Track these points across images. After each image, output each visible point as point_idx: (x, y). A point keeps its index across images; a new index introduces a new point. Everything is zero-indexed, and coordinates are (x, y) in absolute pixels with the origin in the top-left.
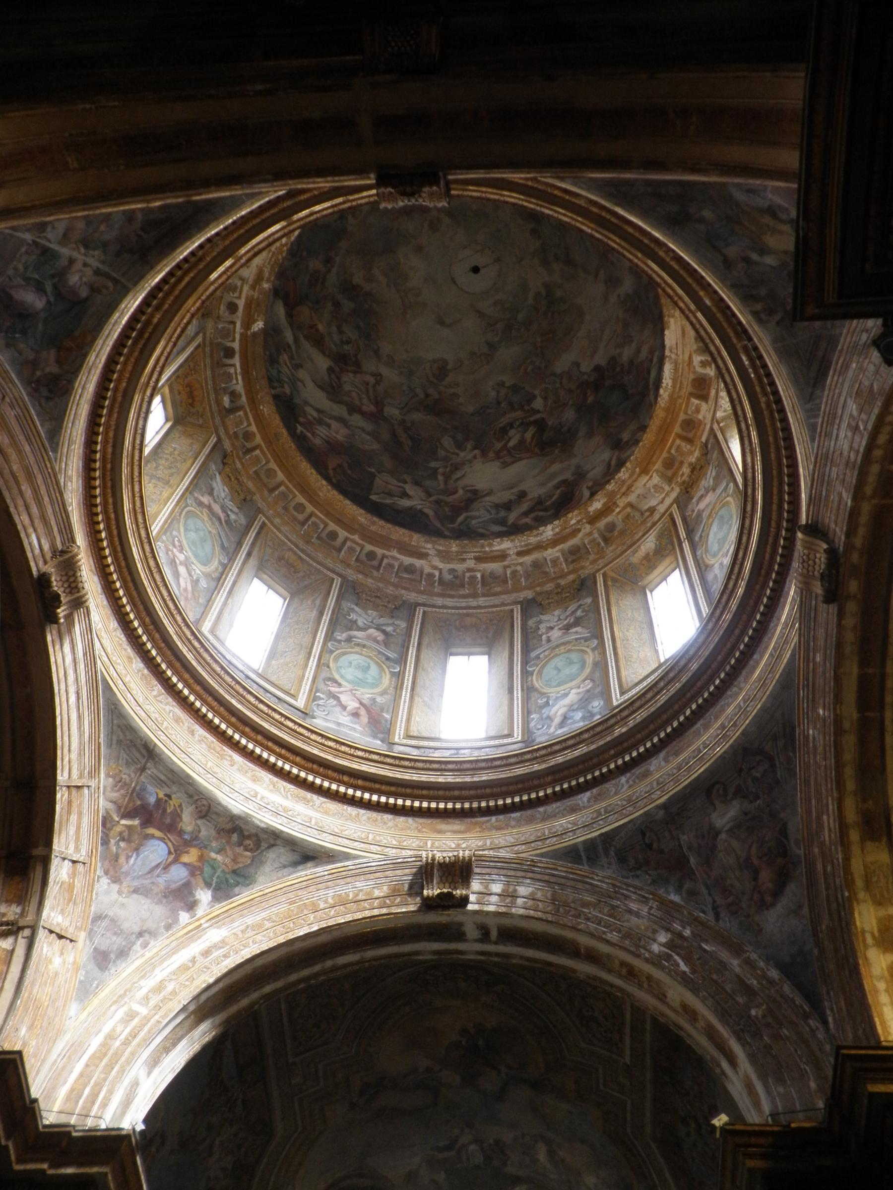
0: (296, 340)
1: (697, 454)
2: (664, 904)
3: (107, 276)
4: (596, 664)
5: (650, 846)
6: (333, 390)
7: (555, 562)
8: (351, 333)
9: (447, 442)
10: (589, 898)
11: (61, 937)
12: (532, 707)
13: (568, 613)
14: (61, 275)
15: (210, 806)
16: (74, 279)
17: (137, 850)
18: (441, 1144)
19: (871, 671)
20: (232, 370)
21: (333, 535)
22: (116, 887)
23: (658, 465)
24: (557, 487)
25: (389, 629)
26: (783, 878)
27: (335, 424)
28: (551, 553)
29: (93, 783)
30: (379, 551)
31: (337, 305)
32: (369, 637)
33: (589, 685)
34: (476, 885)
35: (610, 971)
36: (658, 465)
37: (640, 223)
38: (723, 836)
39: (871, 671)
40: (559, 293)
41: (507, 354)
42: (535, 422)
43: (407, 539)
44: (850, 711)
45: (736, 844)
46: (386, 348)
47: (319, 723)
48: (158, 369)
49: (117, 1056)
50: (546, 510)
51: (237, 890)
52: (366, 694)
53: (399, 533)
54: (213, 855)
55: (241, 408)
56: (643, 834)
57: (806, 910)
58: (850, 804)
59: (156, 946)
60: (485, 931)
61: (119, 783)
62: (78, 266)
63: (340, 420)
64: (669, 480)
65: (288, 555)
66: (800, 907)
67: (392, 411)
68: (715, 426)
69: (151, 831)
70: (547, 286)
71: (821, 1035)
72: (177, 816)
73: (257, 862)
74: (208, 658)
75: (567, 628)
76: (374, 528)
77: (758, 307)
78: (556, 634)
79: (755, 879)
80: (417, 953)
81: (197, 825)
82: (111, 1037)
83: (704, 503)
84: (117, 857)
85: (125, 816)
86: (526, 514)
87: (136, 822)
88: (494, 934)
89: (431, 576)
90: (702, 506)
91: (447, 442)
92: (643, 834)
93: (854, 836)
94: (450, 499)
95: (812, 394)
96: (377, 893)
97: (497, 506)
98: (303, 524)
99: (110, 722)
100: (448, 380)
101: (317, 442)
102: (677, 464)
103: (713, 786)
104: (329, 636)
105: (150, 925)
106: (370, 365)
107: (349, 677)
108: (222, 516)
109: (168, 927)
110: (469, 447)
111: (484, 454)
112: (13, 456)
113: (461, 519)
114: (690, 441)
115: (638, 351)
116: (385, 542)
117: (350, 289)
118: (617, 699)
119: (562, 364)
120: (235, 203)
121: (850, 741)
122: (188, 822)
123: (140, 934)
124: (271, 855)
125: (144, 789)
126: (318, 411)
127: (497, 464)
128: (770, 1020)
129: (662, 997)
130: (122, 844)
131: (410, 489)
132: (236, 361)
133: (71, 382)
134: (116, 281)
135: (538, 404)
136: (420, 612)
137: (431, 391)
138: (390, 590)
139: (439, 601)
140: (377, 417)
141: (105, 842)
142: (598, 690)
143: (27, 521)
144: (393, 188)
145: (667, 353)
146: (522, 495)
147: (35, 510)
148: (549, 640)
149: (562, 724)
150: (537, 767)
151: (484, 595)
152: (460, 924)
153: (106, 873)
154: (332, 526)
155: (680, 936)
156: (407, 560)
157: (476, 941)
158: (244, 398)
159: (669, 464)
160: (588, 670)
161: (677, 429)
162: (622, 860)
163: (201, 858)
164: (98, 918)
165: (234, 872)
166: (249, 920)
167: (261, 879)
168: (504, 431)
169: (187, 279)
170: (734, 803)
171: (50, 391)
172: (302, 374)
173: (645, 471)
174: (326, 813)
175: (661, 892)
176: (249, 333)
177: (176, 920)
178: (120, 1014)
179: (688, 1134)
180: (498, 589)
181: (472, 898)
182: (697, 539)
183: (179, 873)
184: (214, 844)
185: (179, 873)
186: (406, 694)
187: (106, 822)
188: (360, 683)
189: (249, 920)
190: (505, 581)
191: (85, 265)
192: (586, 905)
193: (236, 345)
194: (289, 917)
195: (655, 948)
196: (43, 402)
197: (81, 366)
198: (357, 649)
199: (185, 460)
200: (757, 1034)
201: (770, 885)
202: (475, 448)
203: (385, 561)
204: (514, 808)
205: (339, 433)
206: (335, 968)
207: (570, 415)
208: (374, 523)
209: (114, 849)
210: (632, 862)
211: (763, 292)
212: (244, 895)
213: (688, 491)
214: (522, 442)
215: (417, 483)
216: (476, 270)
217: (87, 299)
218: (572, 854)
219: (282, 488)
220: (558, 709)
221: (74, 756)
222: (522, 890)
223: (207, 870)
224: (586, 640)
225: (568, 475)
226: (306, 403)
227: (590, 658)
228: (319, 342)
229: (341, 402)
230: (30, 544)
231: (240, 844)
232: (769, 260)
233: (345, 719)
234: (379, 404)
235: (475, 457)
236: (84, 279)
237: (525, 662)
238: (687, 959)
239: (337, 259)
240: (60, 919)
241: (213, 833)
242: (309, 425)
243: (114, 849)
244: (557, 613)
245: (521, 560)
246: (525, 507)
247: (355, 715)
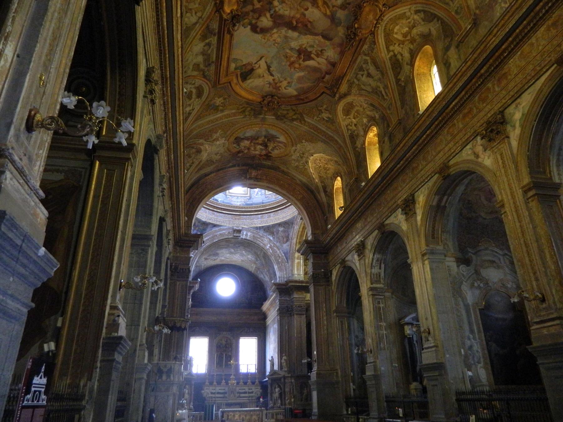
2: (270, 239)
10: (259, 237)
26: (287, 241)
34: (242, 233)
44: (301, 230)
58: (298, 240)
121: (300, 233)
162: (264, 230)
167: (208, 230)
192: (258, 238)
194: (213, 237)
200: (279, 264)
218: (257, 228)
222: (249, 234)
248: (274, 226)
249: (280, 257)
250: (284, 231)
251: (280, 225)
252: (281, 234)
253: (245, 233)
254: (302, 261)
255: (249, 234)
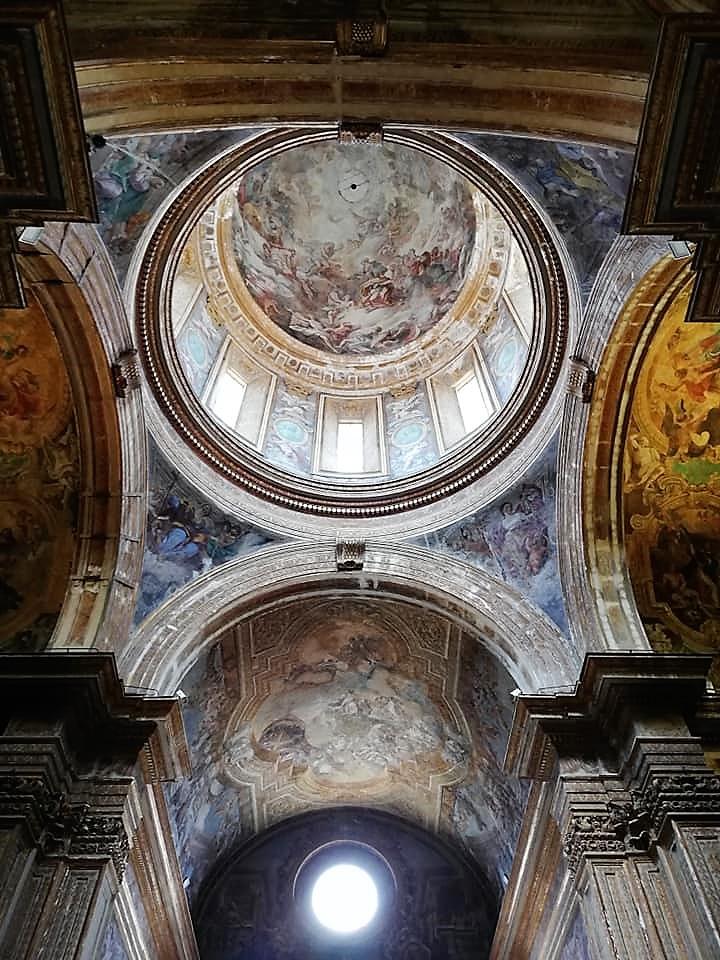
0: (244, 224)
1: (491, 310)
2: (474, 569)
3: (161, 176)
4: (429, 432)
5: (466, 537)
6: (267, 259)
7: (401, 371)
8: (277, 223)
9: (334, 295)
11: (124, 585)
12: (392, 456)
13: (411, 400)
14: (134, 173)
15: (211, 509)
16: (140, 177)
17: (168, 534)
18: (335, 702)
19: (605, 442)
20: (212, 242)
21: (271, 349)
22: (155, 556)
23: (466, 315)
24: (400, 326)
25: (305, 407)
26: (544, 558)
27: (268, 280)
28: (399, 366)
29: (142, 495)
30: (298, 361)
31: (269, 204)
32: (295, 411)
33: (425, 444)
35: (443, 608)
36: (466, 315)
37: (495, 164)
38: (509, 533)
39: (605, 442)
40: (404, 205)
41: (371, 242)
42: (386, 286)
43: (314, 354)
44: (592, 466)
45: (516, 538)
46: (297, 234)
47: (269, 461)
48: (184, 239)
49: (161, 654)
50: (393, 340)
51: (227, 559)
52: (295, 445)
53: (309, 350)
54: (213, 538)
55: (217, 267)
56: (462, 531)
57: (558, 575)
58: (589, 517)
59: (180, 591)
60: (371, 586)
61: (157, 495)
62: (143, 168)
63: (271, 278)
64: (472, 325)
65: (245, 360)
66: (554, 575)
67: (301, 274)
68: (504, 293)
69: (176, 523)
70: (397, 200)
71: (567, 646)
72: (191, 515)
73: (239, 542)
74: (209, 421)
75: (410, 410)
76: (295, 346)
77: (562, 222)
78: (403, 414)
79: (528, 558)
80: (331, 595)
81: (203, 520)
82: (157, 643)
83: (495, 339)
84: (156, 538)
85: (159, 515)
86: (382, 342)
87: (167, 518)
88: (376, 585)
89: (328, 376)
90: (493, 341)
91: (334, 295)
92: (462, 531)
93: (591, 536)
94: (336, 330)
95: (588, 277)
96: (309, 561)
97: (364, 336)
98: (253, 341)
99: (152, 458)
100: (333, 257)
101: (258, 291)
102: (476, 316)
103: (503, 506)
104: (272, 410)
105: (175, 579)
106: (288, 244)
107: (285, 435)
108: (208, 334)
109: (186, 581)
110: (347, 299)
111: (356, 303)
112: (99, 292)
113: (342, 343)
114: (485, 301)
115: (452, 244)
116: (302, 356)
117: (277, 195)
118: (442, 453)
119: (403, 251)
120: (246, 134)
121: (591, 483)
122: (198, 518)
123: (170, 584)
124: (248, 537)
125: (172, 499)
126: (259, 272)
127: (364, 310)
128: (537, 637)
129: (473, 624)
130: (159, 531)
131: (312, 323)
132: (215, 236)
133: (134, 245)
134: (166, 180)
135: (388, 274)
136: (322, 396)
137: (324, 263)
138: (304, 384)
139: (333, 392)
140: (292, 277)
141: (149, 529)
142: (430, 447)
143: (106, 334)
144: (352, 132)
145: (476, 246)
146: (379, 330)
147: (110, 325)
148: (399, 418)
149: (410, 466)
150: (398, 491)
151: (360, 389)
152: (357, 579)
153: (150, 548)
154: (271, 344)
155: (485, 589)
156: (315, 367)
157: (366, 589)
158: (219, 261)
159: (472, 315)
160: (424, 436)
161: (479, 294)
163: (205, 540)
164: (146, 574)
165: (225, 548)
166: (234, 576)
168: (368, 290)
169: (205, 182)
170: (517, 514)
171: (121, 250)
172: (248, 247)
173: (457, 319)
174: (277, 514)
175: (472, 563)
176: (223, 218)
177: (192, 576)
178: (160, 631)
179: (479, 698)
180: (367, 386)
181: (365, 565)
182: (490, 360)
183: (192, 548)
184: (214, 532)
185: (192, 548)
186: (318, 445)
187: (150, 517)
188: (293, 439)
189: (234, 576)
190: (372, 381)
191: (148, 168)
193: (215, 227)
195: (470, 595)
196: (116, 256)
197: (140, 235)
198: (289, 418)
199: (186, 299)
200: (531, 644)
201: (536, 562)
202: (350, 300)
203: (302, 366)
204: (385, 513)
205: (270, 286)
206: (284, 603)
207: (408, 281)
208: (295, 343)
209: (154, 534)
210: (455, 546)
211: (566, 214)
212: (233, 561)
213: (484, 331)
214: (378, 297)
215: (316, 320)
216: (354, 187)
217: (147, 191)
218: (421, 541)
219: (241, 318)
220: (408, 458)
221: (132, 478)
222: (392, 561)
223: (209, 547)
224: (422, 418)
225: (406, 320)
226: (252, 266)
227: (425, 429)
228: (258, 228)
229: (270, 266)
230: (108, 347)
231: (229, 531)
232: (574, 193)
233: (285, 459)
234: (293, 269)
235: (350, 305)
236: (147, 178)
237: (386, 430)
238: (488, 602)
239: (270, 174)
240: (124, 575)
241: (213, 525)
242: (252, 280)
243: (154, 534)
244: (403, 401)
245: (381, 368)
246: (381, 337)
247: (290, 457)
248: (482, 517)
249: (526, 621)
250: (524, 527)
251: (502, 505)
252: (513, 542)
253: (378, 559)
254: (626, 605)
255: (394, 560)
